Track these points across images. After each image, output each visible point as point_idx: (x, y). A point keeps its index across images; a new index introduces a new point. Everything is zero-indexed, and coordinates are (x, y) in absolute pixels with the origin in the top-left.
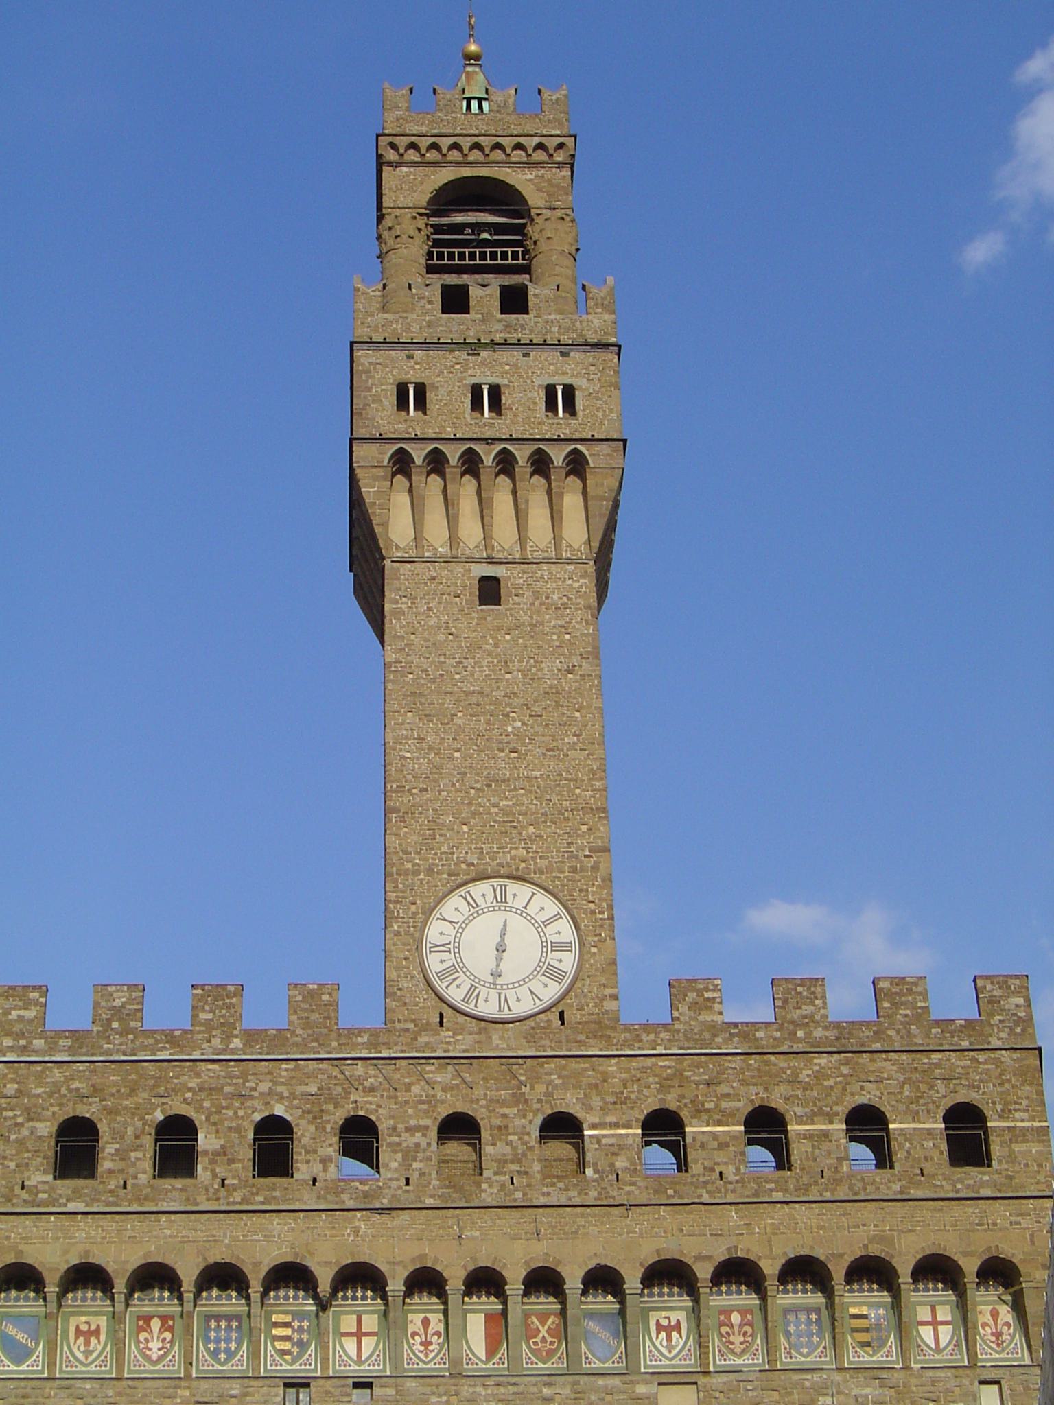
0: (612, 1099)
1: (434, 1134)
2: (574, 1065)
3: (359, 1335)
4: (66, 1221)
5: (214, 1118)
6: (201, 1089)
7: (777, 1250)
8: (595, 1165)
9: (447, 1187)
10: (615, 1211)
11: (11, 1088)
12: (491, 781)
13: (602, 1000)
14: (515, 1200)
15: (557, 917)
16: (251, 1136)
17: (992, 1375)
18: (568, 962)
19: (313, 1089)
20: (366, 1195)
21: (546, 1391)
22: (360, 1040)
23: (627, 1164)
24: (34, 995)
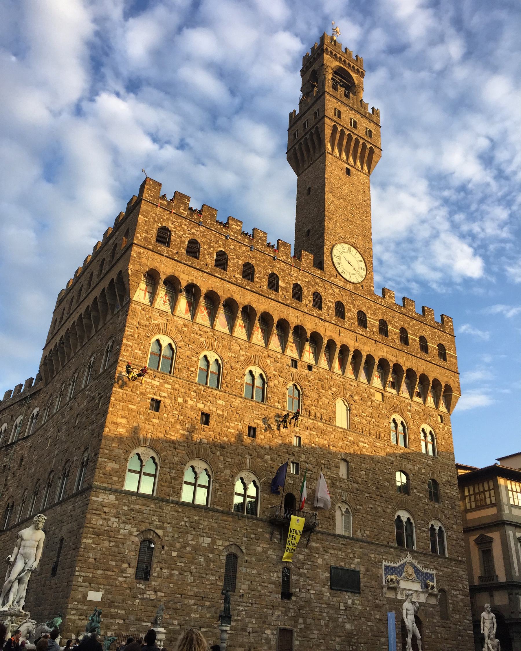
1: (334, 304)
3: (309, 352)
4: (246, 291)
5: (284, 278)
6: (281, 269)
7: (406, 365)
8: (369, 328)
10: (373, 342)
11: (232, 247)
12: (348, 219)
15: (361, 261)
16: (292, 287)
17: (441, 414)
18: (364, 273)
19: (307, 280)
24: (239, 223)
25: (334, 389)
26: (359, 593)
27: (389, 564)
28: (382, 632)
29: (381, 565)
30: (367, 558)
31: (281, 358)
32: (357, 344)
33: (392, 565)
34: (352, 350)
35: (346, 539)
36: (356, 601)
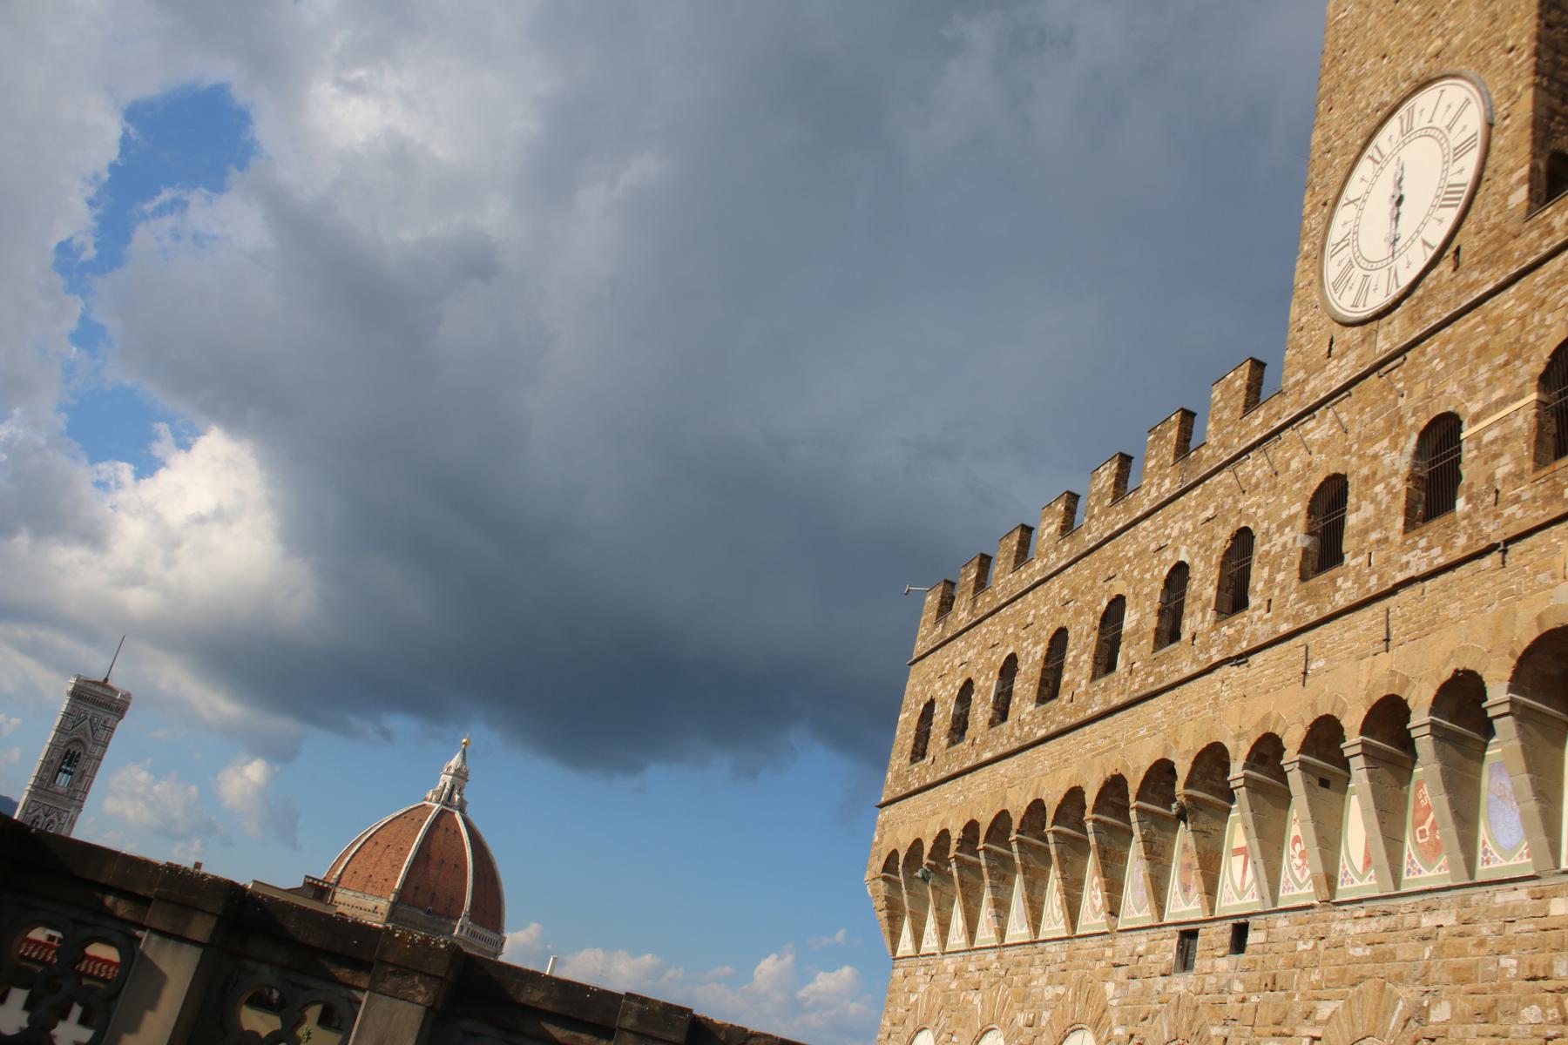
0: (1501, 359)
2: (1461, 327)
9: (1301, 600)
10: (1487, 562)
13: (1506, 196)
14: (1369, 590)
19: (1209, 513)
20: (1233, 641)
21: (1427, 922)
22: (1258, 421)
23: (1507, 469)
25: (1324, 1010)
31: (1148, 951)
32: (1385, 661)
34: (1352, 722)
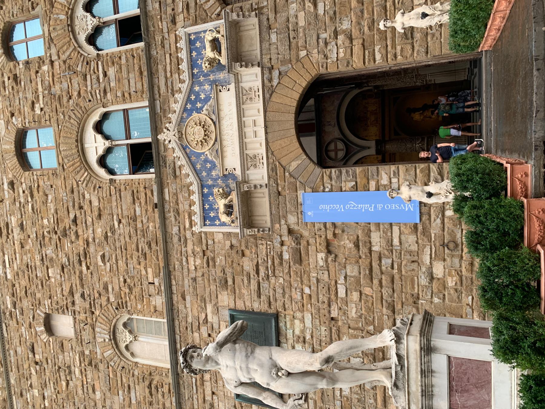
26: (277, 316)
27: (196, 208)
28: (357, 246)
29: (206, 233)
30: (199, 279)
33: (195, 198)
35: (175, 342)
36: (297, 332)
